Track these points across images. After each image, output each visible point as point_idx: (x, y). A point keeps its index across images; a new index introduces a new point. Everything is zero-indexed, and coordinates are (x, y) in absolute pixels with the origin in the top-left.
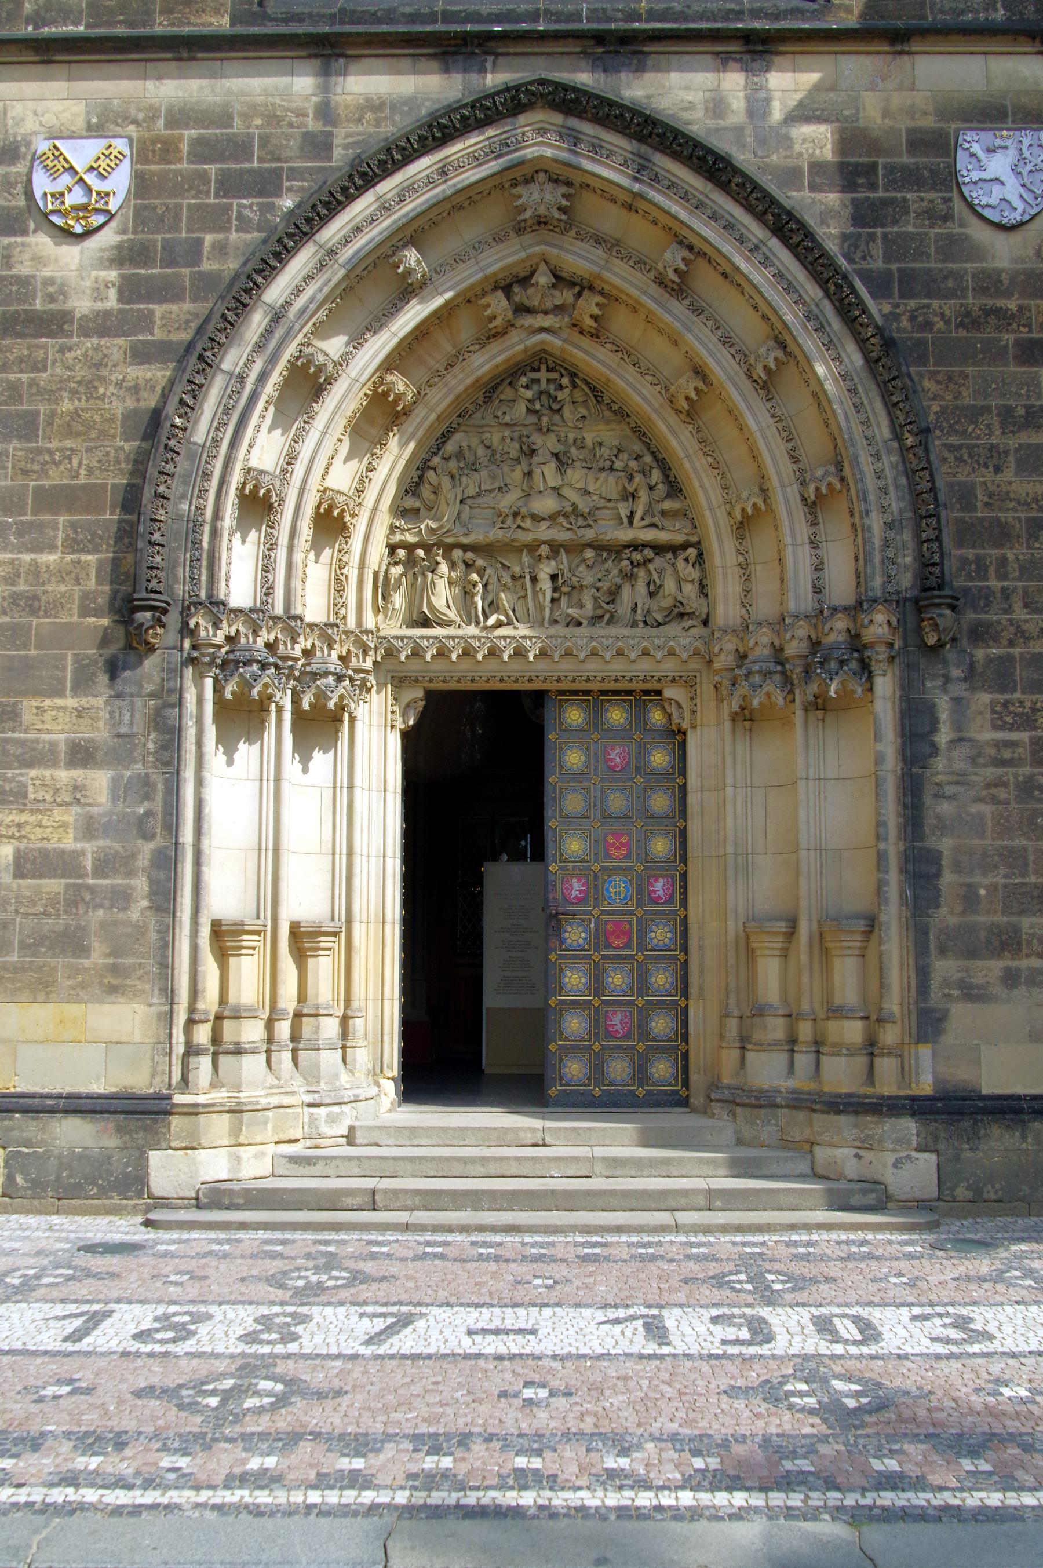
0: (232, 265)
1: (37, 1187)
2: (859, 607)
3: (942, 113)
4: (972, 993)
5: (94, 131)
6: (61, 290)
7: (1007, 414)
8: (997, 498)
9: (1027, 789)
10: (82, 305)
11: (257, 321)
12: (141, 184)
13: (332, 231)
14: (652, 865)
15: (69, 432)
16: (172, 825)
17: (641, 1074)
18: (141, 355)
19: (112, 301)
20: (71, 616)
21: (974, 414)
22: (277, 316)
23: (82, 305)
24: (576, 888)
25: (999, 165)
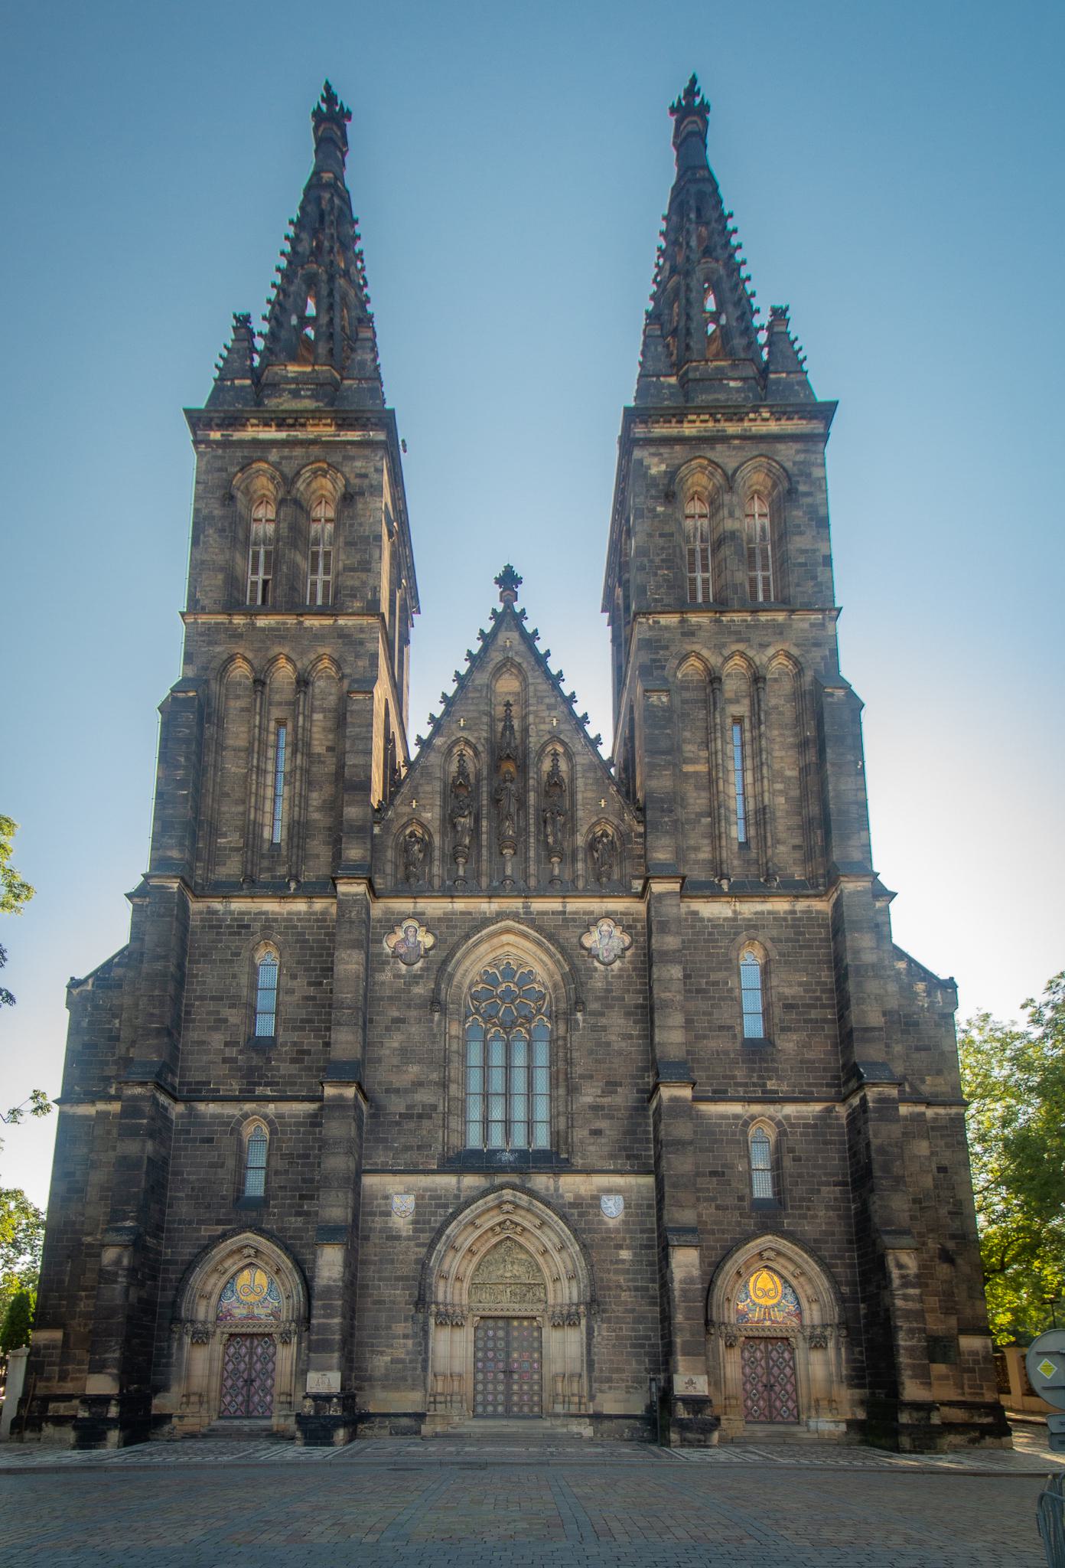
0: (438, 1225)
1: (397, 1434)
2: (578, 1305)
3: (599, 1191)
4: (601, 1391)
5: (407, 1192)
6: (400, 1230)
7: (611, 1261)
8: (609, 1280)
9: (614, 1346)
10: (404, 1234)
11: (444, 1237)
12: (417, 1206)
13: (460, 1218)
14: (521, 1325)
15: (402, 1263)
16: (426, 1352)
17: (531, 1411)
18: (418, 1245)
19: (411, 1233)
20: (402, 1305)
21: (604, 1261)
22: (448, 1237)
23: (404, 1234)
24: (516, 1365)
25: (610, 1204)
